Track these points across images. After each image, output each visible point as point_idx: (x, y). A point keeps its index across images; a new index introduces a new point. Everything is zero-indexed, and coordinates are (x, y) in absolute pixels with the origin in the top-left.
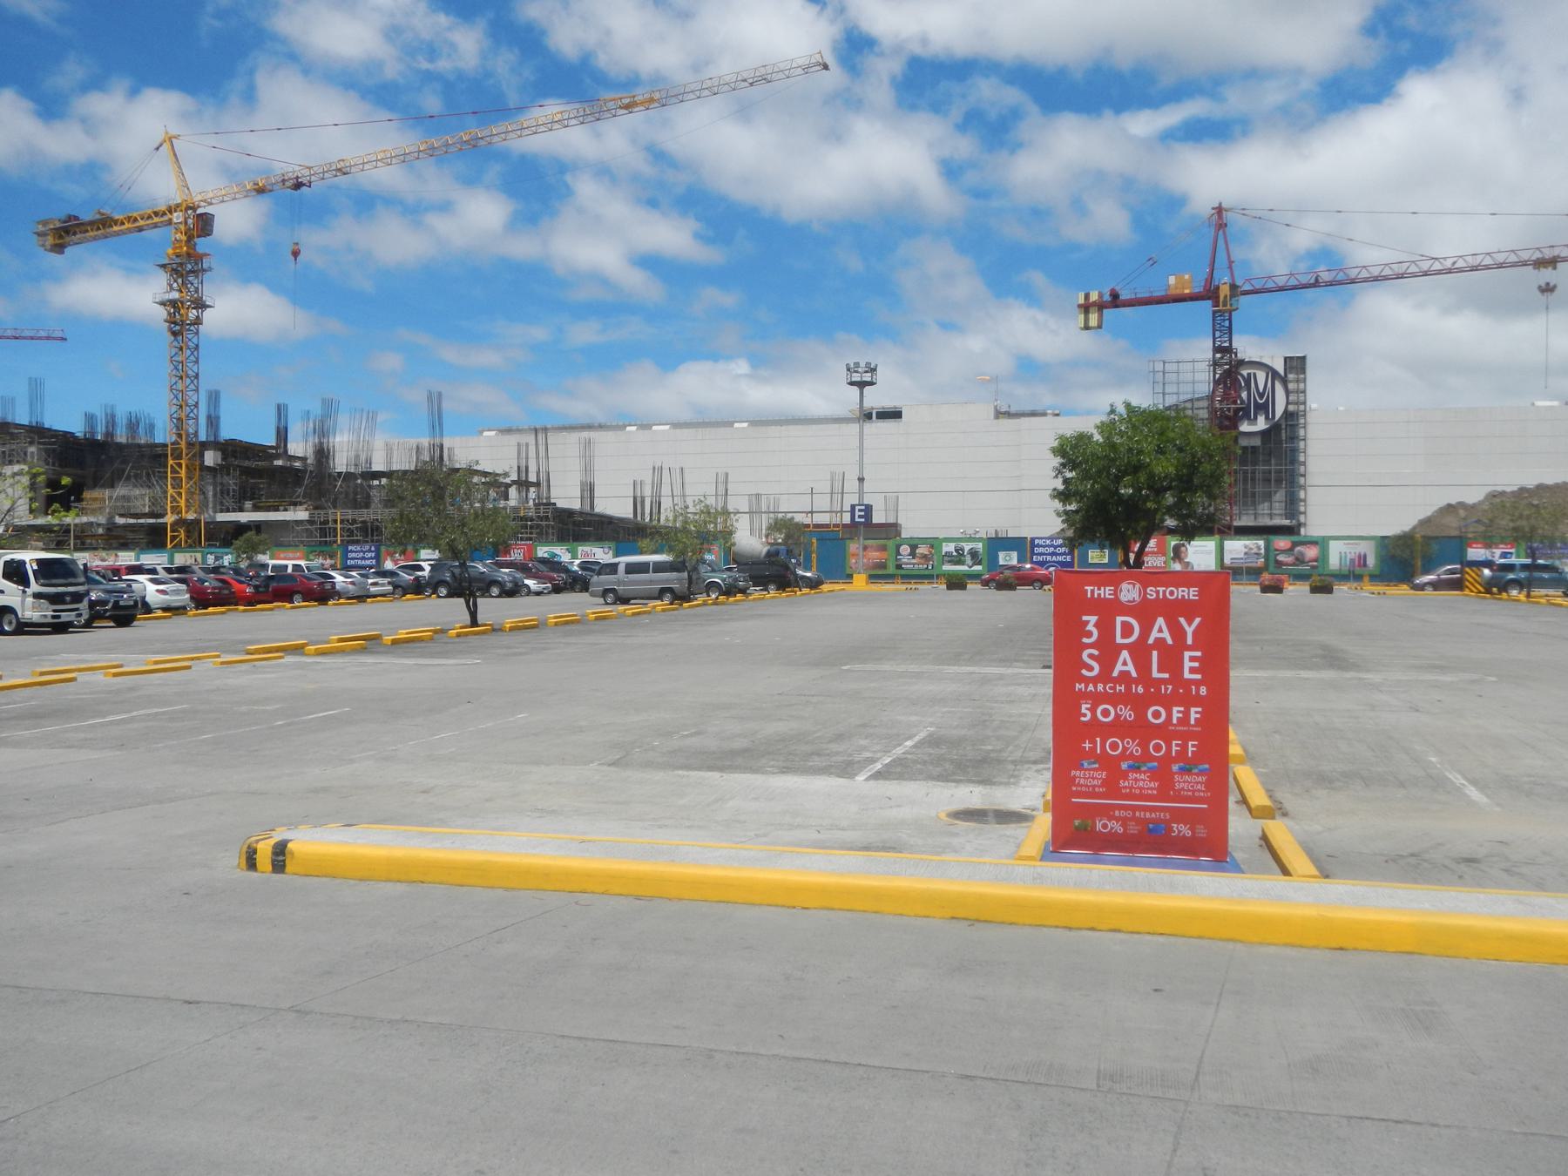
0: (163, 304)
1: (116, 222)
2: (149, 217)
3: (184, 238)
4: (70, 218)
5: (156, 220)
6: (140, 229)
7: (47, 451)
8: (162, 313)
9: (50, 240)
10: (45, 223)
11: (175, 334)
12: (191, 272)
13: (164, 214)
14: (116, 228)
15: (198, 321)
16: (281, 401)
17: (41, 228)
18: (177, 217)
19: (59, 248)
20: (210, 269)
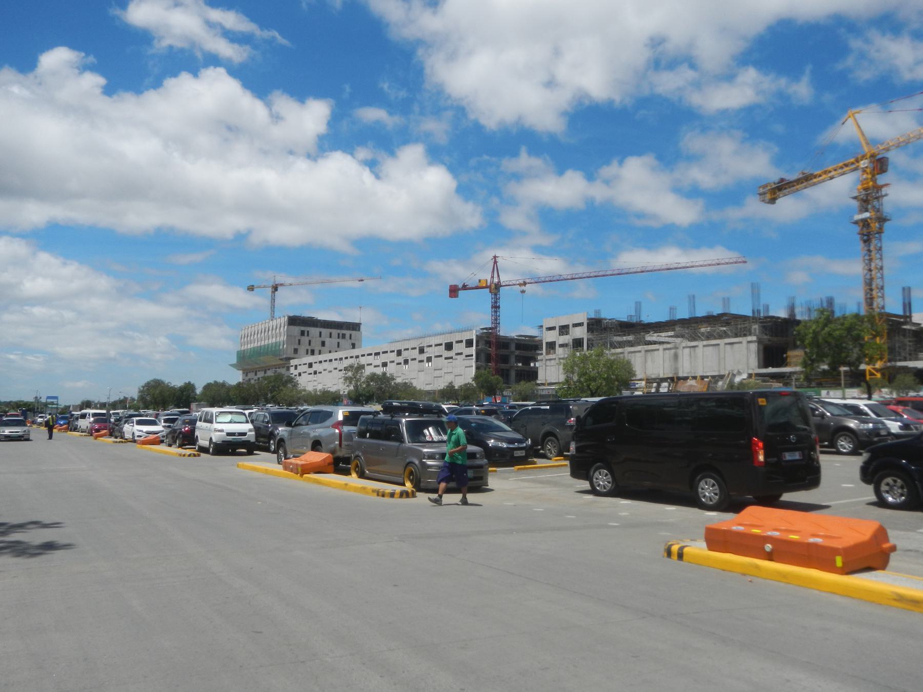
0: (856, 223)
1: (815, 177)
2: (841, 168)
3: (870, 176)
4: (782, 180)
5: (846, 169)
6: (832, 178)
7: (764, 327)
8: (857, 229)
9: (768, 196)
10: (765, 186)
11: (865, 241)
12: (877, 198)
13: (853, 163)
14: (815, 180)
15: (880, 231)
16: (905, 285)
17: (761, 190)
18: (863, 164)
19: (773, 201)
20: (886, 195)
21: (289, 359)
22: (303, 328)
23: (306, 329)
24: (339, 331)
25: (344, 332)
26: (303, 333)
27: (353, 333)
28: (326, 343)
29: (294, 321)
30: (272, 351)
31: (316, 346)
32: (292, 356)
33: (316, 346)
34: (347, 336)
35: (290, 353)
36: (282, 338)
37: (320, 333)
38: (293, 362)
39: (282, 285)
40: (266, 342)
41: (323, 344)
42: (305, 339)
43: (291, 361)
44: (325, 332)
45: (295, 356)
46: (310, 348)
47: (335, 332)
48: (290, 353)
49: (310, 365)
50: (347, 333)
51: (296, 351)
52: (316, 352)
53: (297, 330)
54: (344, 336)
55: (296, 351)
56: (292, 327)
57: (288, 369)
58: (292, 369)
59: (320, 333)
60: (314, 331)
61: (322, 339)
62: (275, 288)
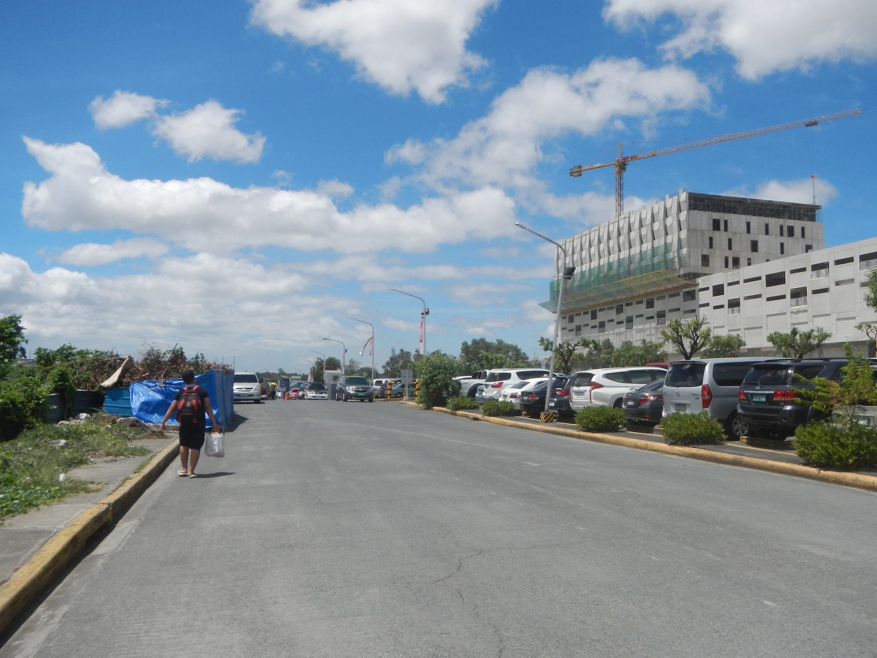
21: (697, 275)
22: (716, 215)
23: (721, 216)
24: (781, 221)
25: (791, 222)
26: (716, 225)
27: (807, 224)
28: (760, 245)
29: (697, 202)
30: (660, 262)
31: (742, 249)
32: (700, 269)
33: (742, 249)
34: (797, 232)
35: (695, 264)
36: (672, 239)
37: (748, 224)
38: (701, 282)
39: (634, 158)
40: (624, 254)
41: (754, 246)
42: (721, 238)
43: (699, 280)
44: (757, 222)
45: (706, 270)
46: (730, 255)
47: (774, 223)
48: (695, 264)
49: (776, 279)
50: (797, 224)
51: (705, 260)
52: (743, 261)
53: (704, 218)
54: (791, 231)
55: (705, 260)
56: (692, 212)
57: (691, 296)
58: (704, 297)
59: (748, 224)
60: (737, 221)
61: (752, 237)
62: (622, 166)
